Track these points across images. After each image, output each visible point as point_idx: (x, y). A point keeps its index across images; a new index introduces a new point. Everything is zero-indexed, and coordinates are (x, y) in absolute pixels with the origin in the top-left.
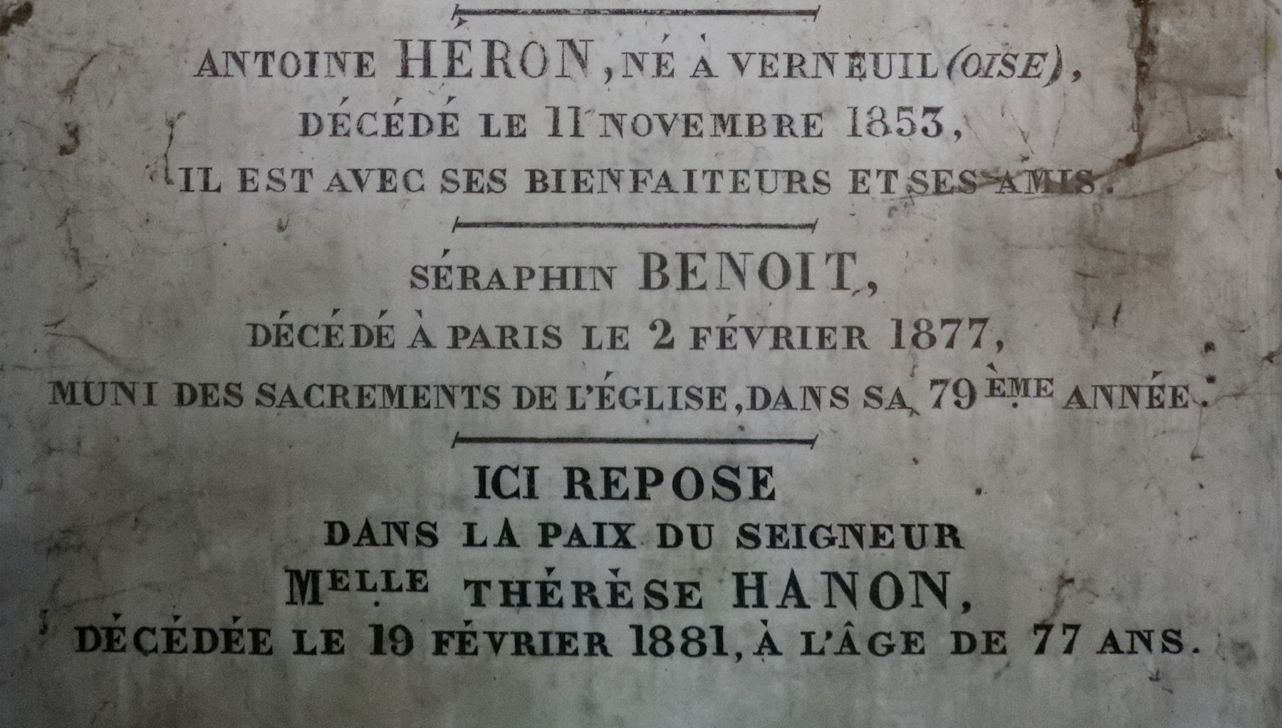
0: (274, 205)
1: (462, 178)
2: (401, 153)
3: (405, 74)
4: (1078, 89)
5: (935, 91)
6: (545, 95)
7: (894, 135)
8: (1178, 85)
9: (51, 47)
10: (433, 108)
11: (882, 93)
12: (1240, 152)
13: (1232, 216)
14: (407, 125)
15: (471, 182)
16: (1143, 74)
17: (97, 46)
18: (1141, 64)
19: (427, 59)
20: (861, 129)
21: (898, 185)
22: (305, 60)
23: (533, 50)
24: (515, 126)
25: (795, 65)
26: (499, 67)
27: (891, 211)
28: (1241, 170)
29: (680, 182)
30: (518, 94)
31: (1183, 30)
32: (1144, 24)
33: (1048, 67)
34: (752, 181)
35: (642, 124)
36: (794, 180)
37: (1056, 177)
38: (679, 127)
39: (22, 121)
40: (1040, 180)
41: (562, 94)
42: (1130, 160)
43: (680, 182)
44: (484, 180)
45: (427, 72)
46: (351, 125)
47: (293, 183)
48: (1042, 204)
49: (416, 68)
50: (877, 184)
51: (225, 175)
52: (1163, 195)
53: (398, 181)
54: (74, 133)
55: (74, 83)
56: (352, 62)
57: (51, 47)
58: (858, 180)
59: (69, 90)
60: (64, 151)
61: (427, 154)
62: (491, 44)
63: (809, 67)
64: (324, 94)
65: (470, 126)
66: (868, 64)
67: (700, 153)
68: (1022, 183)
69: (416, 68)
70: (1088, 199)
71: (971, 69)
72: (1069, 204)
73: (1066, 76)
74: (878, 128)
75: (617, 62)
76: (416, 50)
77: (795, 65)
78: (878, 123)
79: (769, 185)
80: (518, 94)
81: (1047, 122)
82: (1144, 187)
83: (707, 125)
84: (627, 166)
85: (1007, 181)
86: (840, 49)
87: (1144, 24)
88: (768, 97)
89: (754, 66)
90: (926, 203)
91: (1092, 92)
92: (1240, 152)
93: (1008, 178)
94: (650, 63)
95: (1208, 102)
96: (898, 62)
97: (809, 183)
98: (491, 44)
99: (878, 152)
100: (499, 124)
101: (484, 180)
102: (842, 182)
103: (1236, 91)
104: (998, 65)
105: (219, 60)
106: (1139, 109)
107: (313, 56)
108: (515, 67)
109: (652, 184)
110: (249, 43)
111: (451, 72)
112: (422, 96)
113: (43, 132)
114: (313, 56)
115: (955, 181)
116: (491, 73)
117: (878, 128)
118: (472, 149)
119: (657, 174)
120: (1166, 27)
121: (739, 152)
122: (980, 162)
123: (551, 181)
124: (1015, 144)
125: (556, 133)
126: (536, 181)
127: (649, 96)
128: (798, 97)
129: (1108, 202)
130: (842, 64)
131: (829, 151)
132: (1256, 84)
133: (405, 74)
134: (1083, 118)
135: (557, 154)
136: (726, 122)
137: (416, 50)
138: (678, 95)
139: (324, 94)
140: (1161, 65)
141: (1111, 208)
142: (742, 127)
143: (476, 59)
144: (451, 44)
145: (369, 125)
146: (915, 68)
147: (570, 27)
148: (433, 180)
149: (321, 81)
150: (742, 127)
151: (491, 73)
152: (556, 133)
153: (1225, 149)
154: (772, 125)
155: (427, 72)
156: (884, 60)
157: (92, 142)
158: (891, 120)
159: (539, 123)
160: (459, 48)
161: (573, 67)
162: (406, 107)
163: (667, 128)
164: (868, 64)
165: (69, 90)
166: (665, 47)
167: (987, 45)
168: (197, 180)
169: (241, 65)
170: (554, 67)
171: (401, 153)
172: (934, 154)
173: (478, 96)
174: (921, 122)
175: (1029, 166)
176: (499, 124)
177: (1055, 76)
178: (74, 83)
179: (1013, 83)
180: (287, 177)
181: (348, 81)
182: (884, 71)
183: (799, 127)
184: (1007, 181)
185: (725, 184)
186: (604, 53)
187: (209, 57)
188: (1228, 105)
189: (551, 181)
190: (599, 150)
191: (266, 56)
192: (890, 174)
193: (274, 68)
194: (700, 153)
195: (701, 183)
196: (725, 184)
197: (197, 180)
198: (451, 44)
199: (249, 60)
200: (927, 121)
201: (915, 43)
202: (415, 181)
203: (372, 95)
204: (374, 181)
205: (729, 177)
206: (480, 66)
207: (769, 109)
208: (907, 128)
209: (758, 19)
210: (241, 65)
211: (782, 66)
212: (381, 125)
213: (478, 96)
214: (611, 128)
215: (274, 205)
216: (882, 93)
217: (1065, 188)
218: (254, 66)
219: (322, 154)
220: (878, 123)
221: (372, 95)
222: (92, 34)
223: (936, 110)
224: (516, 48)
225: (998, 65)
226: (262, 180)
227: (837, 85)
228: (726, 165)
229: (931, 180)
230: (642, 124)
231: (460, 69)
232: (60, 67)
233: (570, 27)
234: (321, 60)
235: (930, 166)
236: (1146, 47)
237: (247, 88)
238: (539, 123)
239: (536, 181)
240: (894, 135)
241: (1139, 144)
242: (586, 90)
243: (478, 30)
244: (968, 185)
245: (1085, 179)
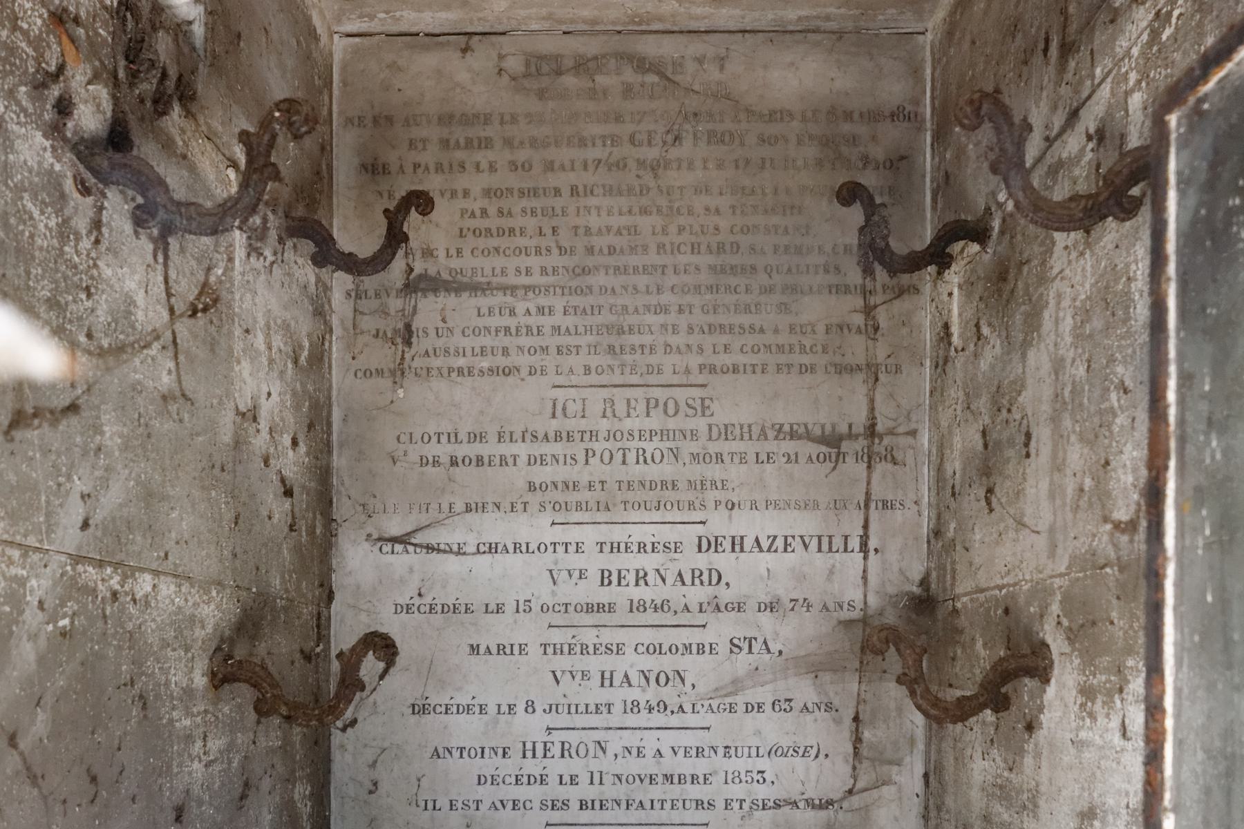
0: (465, 816)
1: (549, 804)
2: (522, 792)
3: (524, 757)
4: (827, 762)
5: (763, 763)
6: (587, 766)
7: (744, 783)
8: (872, 760)
9: (366, 746)
10: (537, 772)
11: (738, 764)
12: (900, 790)
13: (896, 819)
14: (525, 780)
15: (553, 806)
16: (856, 752)
17: (386, 744)
18: (855, 748)
19: (534, 750)
20: (729, 781)
21: (746, 806)
22: (479, 751)
23: (582, 746)
24: (573, 780)
25: (699, 752)
26: (566, 753)
27: (743, 818)
28: (900, 798)
29: (647, 805)
30: (574, 766)
31: (875, 735)
32: (857, 729)
33: (813, 752)
34: (680, 804)
35: (631, 779)
36: (699, 804)
37: (817, 802)
38: (647, 780)
39: (351, 778)
40: (810, 803)
41: (595, 765)
42: (850, 792)
43: (647, 805)
44: (559, 805)
45: (534, 756)
46: (500, 780)
47: (473, 806)
48: (810, 814)
49: (529, 754)
50: (736, 805)
51: (443, 803)
52: (866, 809)
53: (521, 805)
54: (375, 784)
55: (375, 762)
56: (500, 752)
57: (366, 746)
58: (727, 804)
59: (373, 765)
60: (371, 792)
61: (534, 793)
62: (563, 743)
63: (706, 753)
64: (488, 765)
65: (553, 780)
66: (732, 751)
67: (656, 792)
68: (801, 805)
69: (529, 754)
70: (831, 812)
71: (779, 753)
72: (823, 814)
73: (821, 756)
74: (737, 780)
75: (619, 751)
76: (529, 746)
77: (699, 752)
78: (737, 778)
79: (687, 805)
80: (574, 766)
81: (813, 777)
82: (856, 806)
83: (660, 779)
84: (623, 798)
85: (795, 804)
86: (720, 744)
87: (857, 729)
88: (687, 766)
89: (681, 753)
90: (758, 814)
91: (833, 764)
92: (900, 790)
93: (795, 802)
94: (634, 751)
95: (886, 768)
96: (746, 750)
97: (706, 805)
98: (563, 743)
99: (737, 791)
100: (566, 779)
101: (559, 805)
102: (720, 804)
103: (899, 763)
104: (791, 751)
105: (441, 751)
106: (854, 768)
107: (483, 749)
108: (574, 754)
109: (635, 806)
110: (454, 743)
111: (545, 756)
112: (532, 767)
113: (361, 784)
114: (483, 749)
115: (771, 804)
116: (563, 756)
117: (737, 780)
118: (554, 790)
119: (637, 801)
120: (867, 735)
121: (674, 791)
122: (783, 795)
123: (590, 805)
124: (799, 787)
125: (592, 783)
126: (583, 805)
127: (633, 766)
128: (701, 766)
129: (841, 813)
130: (721, 751)
131: (715, 791)
132: (908, 759)
133: (524, 757)
134: (829, 776)
135: (591, 793)
136: (668, 778)
137: (529, 746)
138: (647, 766)
139: (488, 765)
140: (865, 752)
141: (841, 815)
142: (676, 780)
143: (556, 750)
144: (545, 743)
145: (508, 780)
146: (754, 753)
147: (598, 735)
148: (537, 805)
149: (486, 760)
150: (676, 780)
151: (563, 756)
152: (592, 783)
153: (893, 789)
154: (689, 779)
155: (534, 756)
156: (739, 749)
157: (384, 788)
158: (743, 776)
159: (584, 778)
160: (549, 745)
161: (600, 753)
162: (525, 772)
163: (642, 781)
164: (732, 751)
165: (373, 765)
166: (642, 744)
167: (785, 742)
168: (430, 805)
169: (450, 753)
170: (591, 753)
171: (522, 792)
172: (762, 792)
173: (557, 767)
174: (756, 777)
175: (805, 797)
176: (566, 779)
177: (817, 756)
178: (375, 762)
179: (798, 760)
180: (471, 804)
181: (498, 760)
182: (739, 754)
183: (701, 780)
184: (795, 804)
185: (667, 805)
186: (615, 746)
187: (436, 749)
188: (895, 768)
189: (590, 805)
190: (611, 791)
191: (462, 749)
192: (742, 801)
193: (465, 754)
194: (656, 792)
195: (657, 805)
196: (667, 805)
197: (430, 805)
198: (545, 743)
199: (454, 751)
200: (759, 777)
201: (754, 742)
202: (528, 805)
203: (508, 767)
204: (510, 805)
205: (669, 803)
206: (558, 753)
207: (688, 772)
208: (749, 780)
209: (683, 731)
210: (450, 753)
211: (693, 752)
212: (513, 780)
213: (557, 767)
214: (617, 780)
215: (465, 816)
216: (738, 764)
217: (821, 807)
218: (456, 754)
219: (487, 793)
220: (737, 778)
221: (508, 767)
222: (384, 740)
223: (763, 772)
224: (574, 745)
225: (791, 751)
226: (460, 805)
227: (719, 761)
228: (668, 797)
229: (761, 804)
230: (631, 779)
231: (549, 754)
232: (369, 755)
233: (598, 735)
234: (487, 751)
235: (760, 797)
236: (857, 740)
237: (453, 764)
238: (584, 778)
239: (583, 805)
240: (744, 783)
241: (854, 785)
242: (606, 764)
243: (557, 737)
244: (777, 806)
245: (830, 803)
